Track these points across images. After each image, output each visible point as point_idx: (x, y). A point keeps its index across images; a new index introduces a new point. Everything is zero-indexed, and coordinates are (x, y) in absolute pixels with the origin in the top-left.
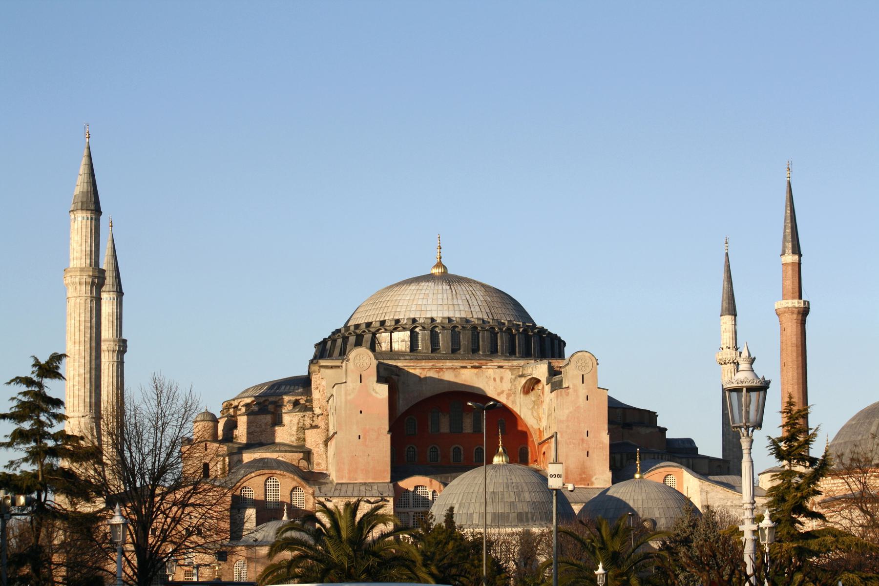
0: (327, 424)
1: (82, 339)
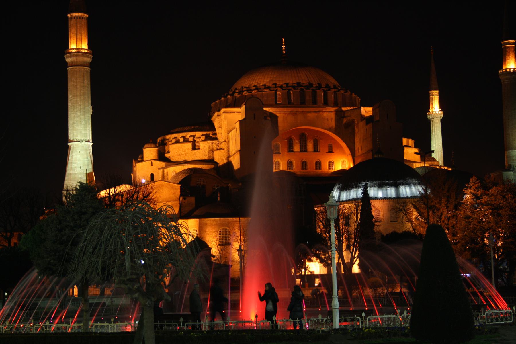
0: (228, 147)
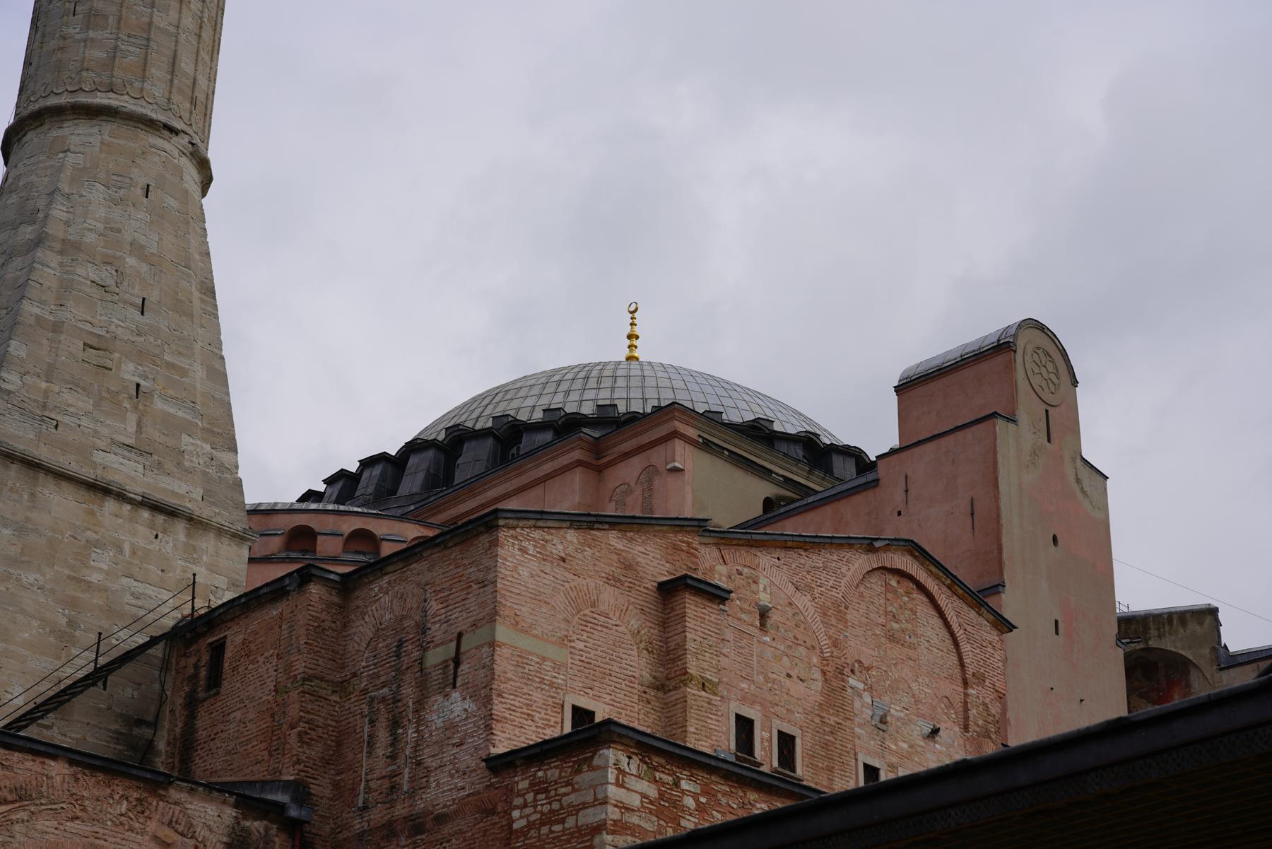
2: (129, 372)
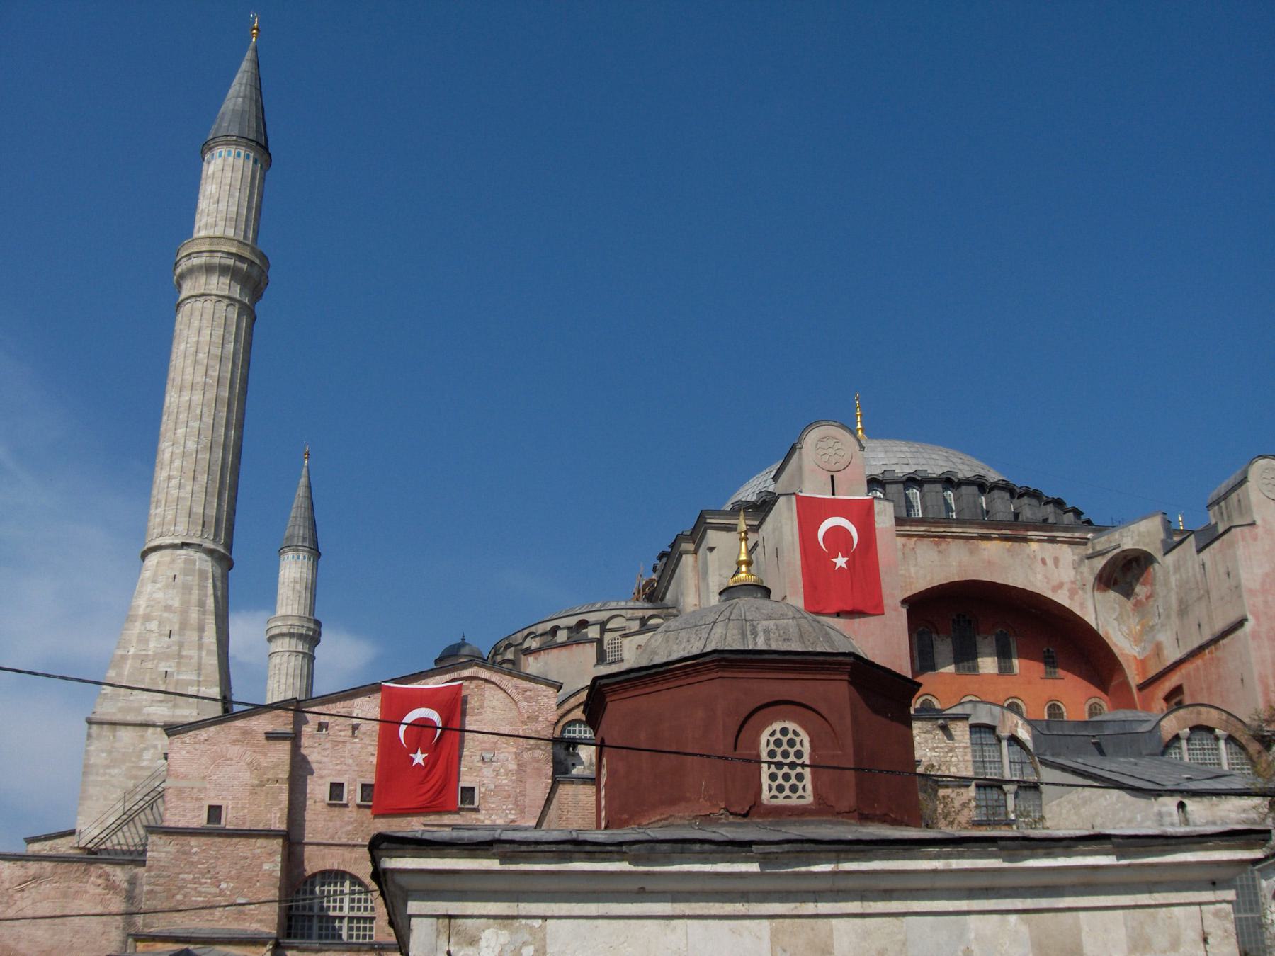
1: (200, 379)
2: (163, 667)
